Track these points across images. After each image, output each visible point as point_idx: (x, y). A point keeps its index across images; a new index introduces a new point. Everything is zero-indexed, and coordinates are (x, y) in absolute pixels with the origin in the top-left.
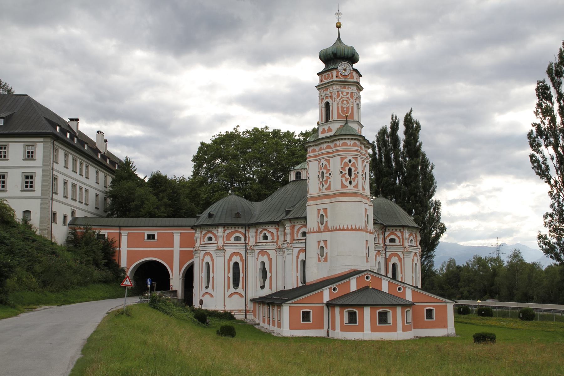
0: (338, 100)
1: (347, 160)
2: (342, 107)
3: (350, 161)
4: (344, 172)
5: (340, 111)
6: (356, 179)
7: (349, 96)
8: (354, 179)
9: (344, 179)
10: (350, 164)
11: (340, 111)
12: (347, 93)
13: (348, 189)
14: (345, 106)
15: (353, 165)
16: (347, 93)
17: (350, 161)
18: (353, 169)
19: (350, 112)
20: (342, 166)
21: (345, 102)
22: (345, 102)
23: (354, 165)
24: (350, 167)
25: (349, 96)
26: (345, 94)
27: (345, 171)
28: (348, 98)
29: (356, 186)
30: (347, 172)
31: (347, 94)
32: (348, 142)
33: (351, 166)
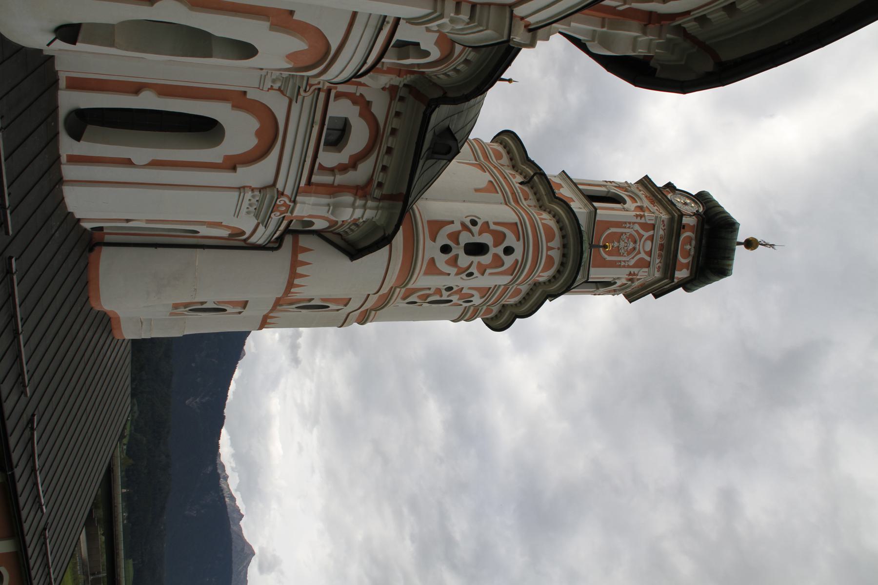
1: (510, 240)
3: (508, 251)
4: (475, 229)
8: (454, 262)
9: (457, 227)
10: (500, 250)
13: (428, 241)
15: (496, 256)
17: (508, 251)
18: (486, 259)
20: (493, 227)
23: (498, 262)
24: (493, 250)
27: (480, 233)
29: (432, 268)
30: (478, 239)
32: (556, 243)
33: (496, 256)
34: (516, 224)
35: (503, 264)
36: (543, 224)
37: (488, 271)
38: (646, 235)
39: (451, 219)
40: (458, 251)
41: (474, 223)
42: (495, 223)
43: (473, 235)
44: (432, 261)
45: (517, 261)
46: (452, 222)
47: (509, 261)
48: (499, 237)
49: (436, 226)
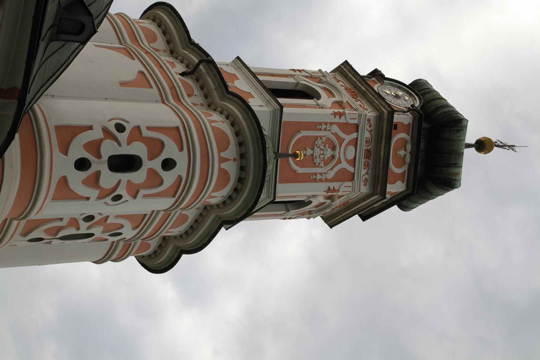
0: (335, 129)
1: (171, 150)
2: (312, 142)
4: (123, 137)
5: (304, 133)
6: (93, 193)
7: (344, 165)
9: (97, 134)
10: (156, 164)
11: (304, 133)
12: (353, 162)
13: (57, 154)
14: (317, 151)
15: (152, 172)
16: (353, 162)
18: (138, 177)
19: (300, 170)
21: (329, 153)
22: (329, 153)
23: (155, 179)
24: (147, 164)
25: (344, 165)
26: (351, 153)
27: (129, 142)
28: (339, 162)
29: (64, 191)
31: (348, 161)
32: (231, 152)
34: (177, 128)
35: (161, 183)
36: (213, 128)
37: (142, 192)
38: (348, 138)
39: (89, 124)
40: (100, 166)
41: (120, 128)
42: (149, 128)
43: (119, 144)
44: (64, 181)
45: (180, 178)
46: (91, 128)
47: (169, 178)
48: (155, 147)
49: (67, 134)
